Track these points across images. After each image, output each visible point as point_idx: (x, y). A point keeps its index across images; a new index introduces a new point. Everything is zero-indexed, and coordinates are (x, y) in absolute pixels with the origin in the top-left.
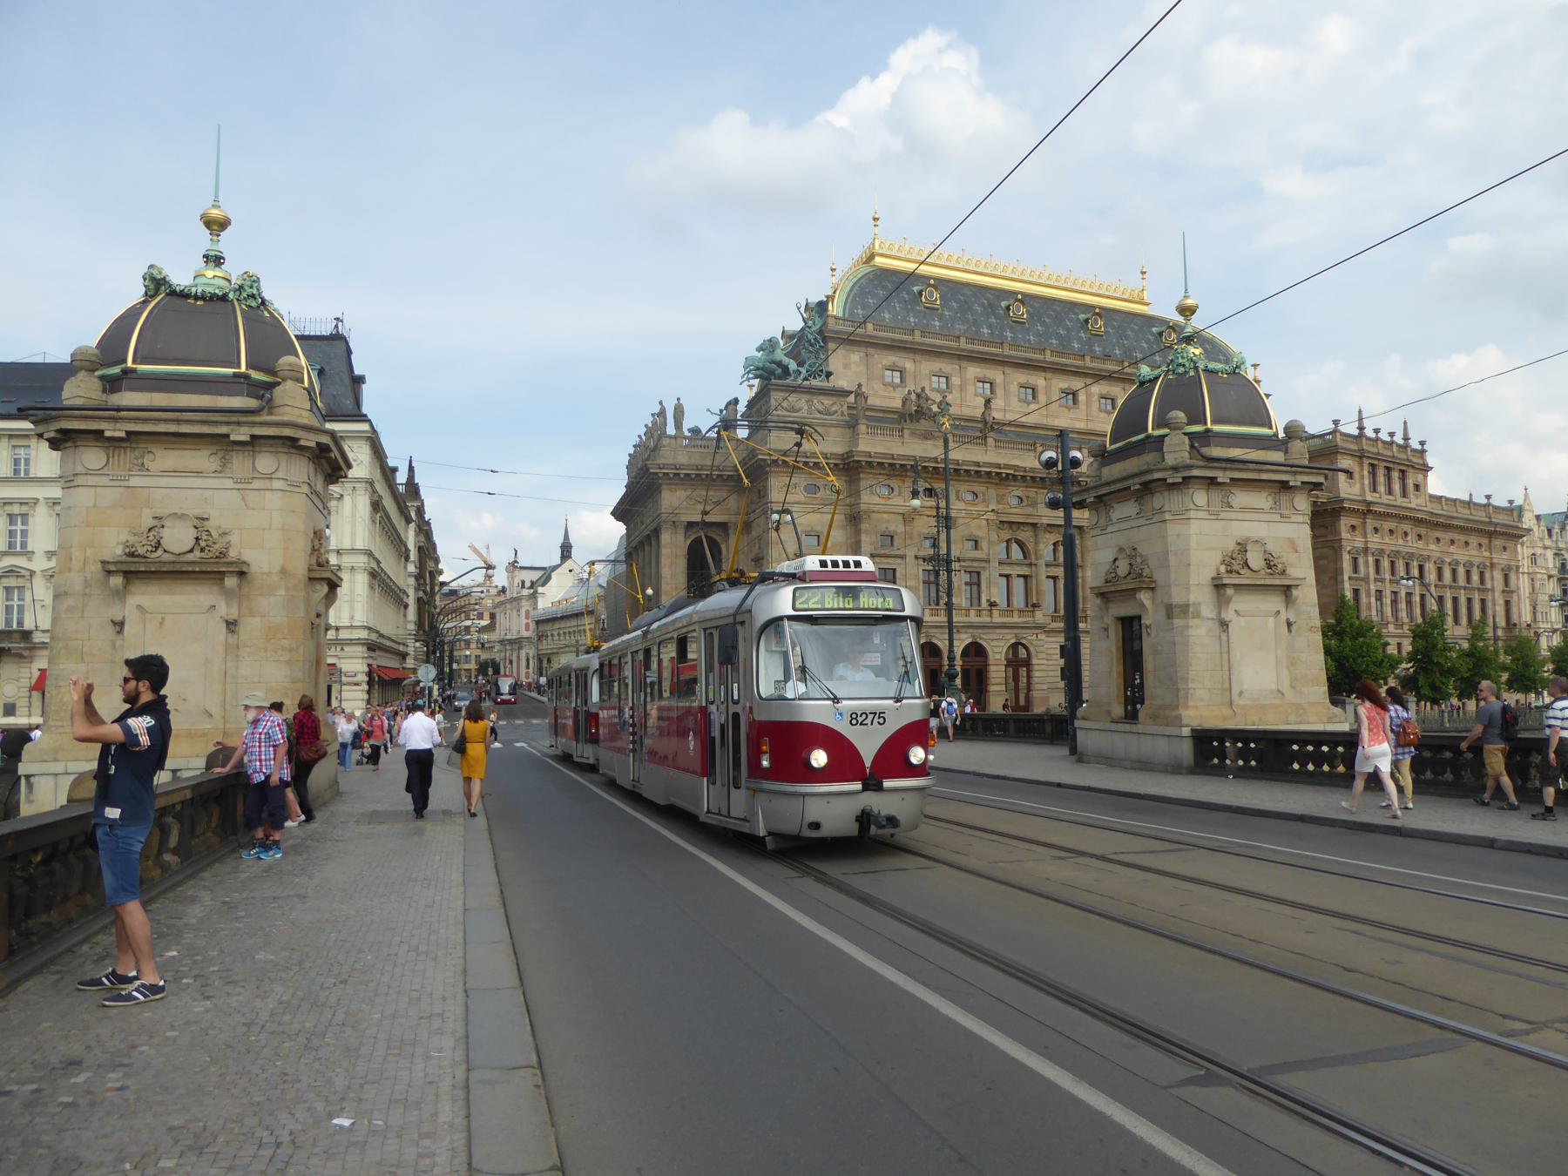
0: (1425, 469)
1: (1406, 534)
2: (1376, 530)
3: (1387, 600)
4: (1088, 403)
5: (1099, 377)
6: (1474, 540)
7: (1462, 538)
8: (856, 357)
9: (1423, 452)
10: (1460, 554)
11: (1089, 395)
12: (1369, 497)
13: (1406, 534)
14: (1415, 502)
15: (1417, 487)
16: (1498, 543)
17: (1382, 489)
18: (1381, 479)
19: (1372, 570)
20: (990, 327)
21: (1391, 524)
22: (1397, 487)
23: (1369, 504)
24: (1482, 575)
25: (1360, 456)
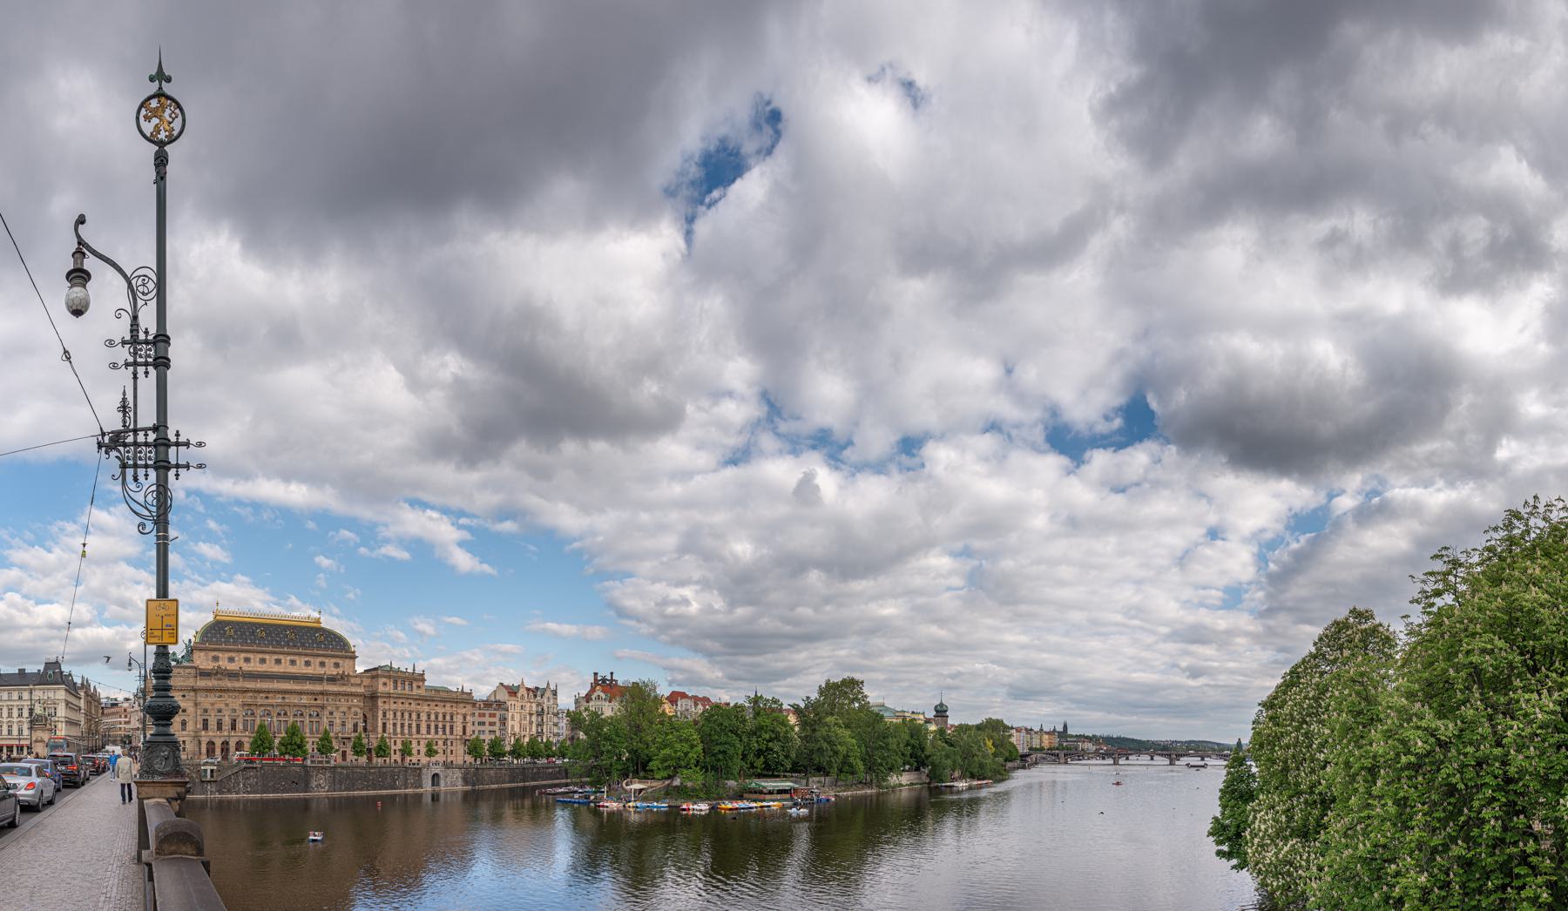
0: (424, 680)
1: (410, 704)
2: (395, 703)
3: (399, 726)
4: (285, 663)
5: (289, 654)
6: (448, 705)
7: (442, 704)
8: (202, 654)
9: (423, 674)
10: (440, 710)
11: (286, 660)
12: (392, 691)
13: (410, 704)
14: (415, 692)
15: (419, 687)
16: (462, 705)
17: (399, 688)
18: (399, 684)
19: (392, 717)
20: (251, 640)
21: (401, 701)
22: (407, 687)
23: (390, 693)
24: (452, 717)
25: (389, 677)
